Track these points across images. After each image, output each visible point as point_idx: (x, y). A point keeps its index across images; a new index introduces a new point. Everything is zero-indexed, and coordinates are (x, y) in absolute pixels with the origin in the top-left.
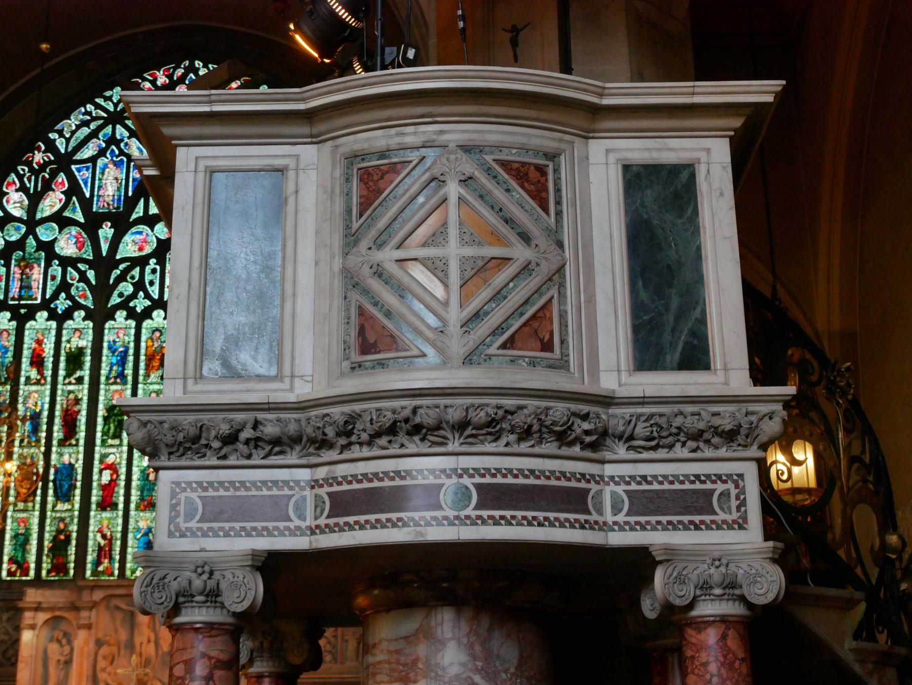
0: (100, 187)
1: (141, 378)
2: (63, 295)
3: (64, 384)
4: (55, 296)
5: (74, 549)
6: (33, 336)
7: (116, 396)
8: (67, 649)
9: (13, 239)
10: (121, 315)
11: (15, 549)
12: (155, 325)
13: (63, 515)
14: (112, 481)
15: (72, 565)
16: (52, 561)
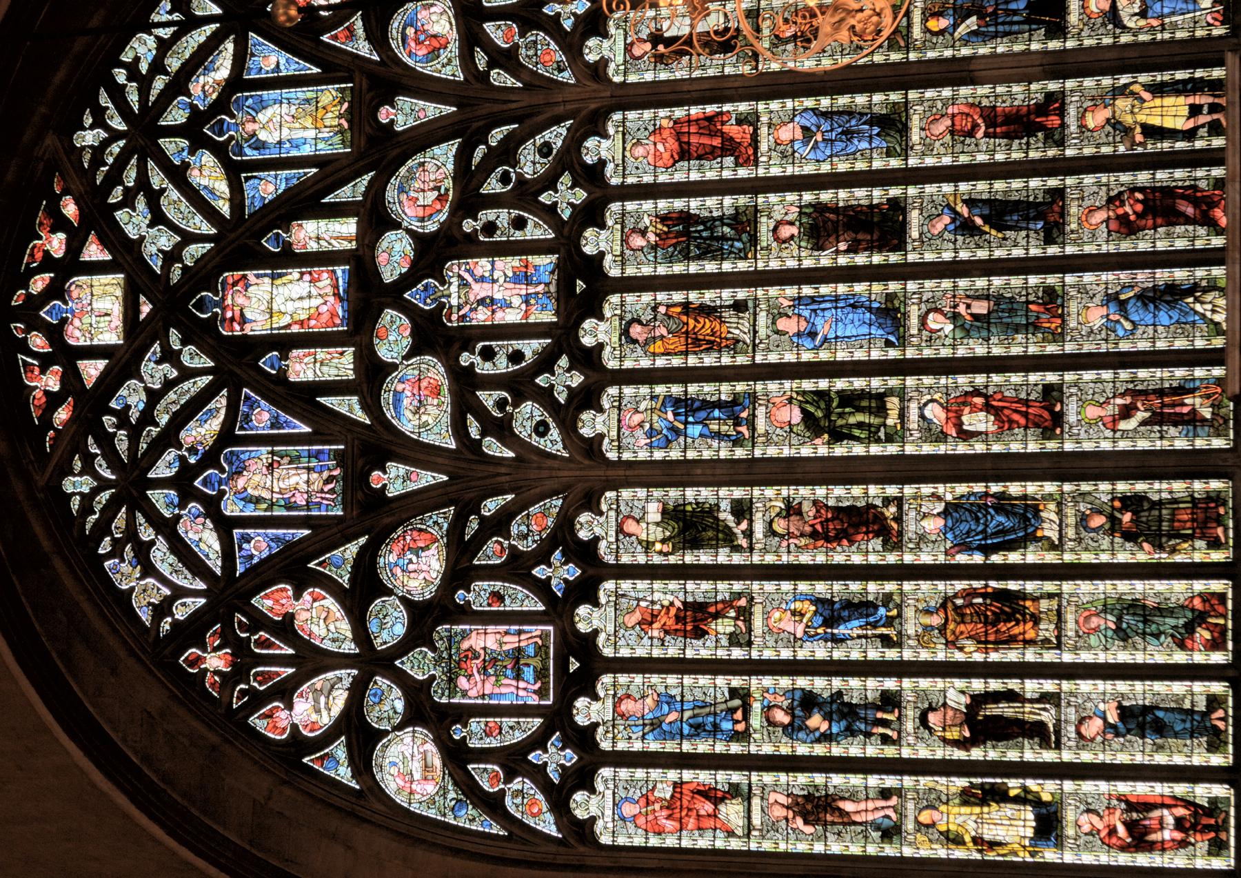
0: (289, 506)
1: (741, 360)
2: (540, 572)
3: (751, 549)
4: (542, 588)
5: (1157, 485)
6: (632, 635)
9: (400, 706)
10: (590, 424)
11: (1157, 636)
12: (615, 339)
13: (1071, 520)
14: (988, 408)
15: (1198, 485)
16: (1186, 538)
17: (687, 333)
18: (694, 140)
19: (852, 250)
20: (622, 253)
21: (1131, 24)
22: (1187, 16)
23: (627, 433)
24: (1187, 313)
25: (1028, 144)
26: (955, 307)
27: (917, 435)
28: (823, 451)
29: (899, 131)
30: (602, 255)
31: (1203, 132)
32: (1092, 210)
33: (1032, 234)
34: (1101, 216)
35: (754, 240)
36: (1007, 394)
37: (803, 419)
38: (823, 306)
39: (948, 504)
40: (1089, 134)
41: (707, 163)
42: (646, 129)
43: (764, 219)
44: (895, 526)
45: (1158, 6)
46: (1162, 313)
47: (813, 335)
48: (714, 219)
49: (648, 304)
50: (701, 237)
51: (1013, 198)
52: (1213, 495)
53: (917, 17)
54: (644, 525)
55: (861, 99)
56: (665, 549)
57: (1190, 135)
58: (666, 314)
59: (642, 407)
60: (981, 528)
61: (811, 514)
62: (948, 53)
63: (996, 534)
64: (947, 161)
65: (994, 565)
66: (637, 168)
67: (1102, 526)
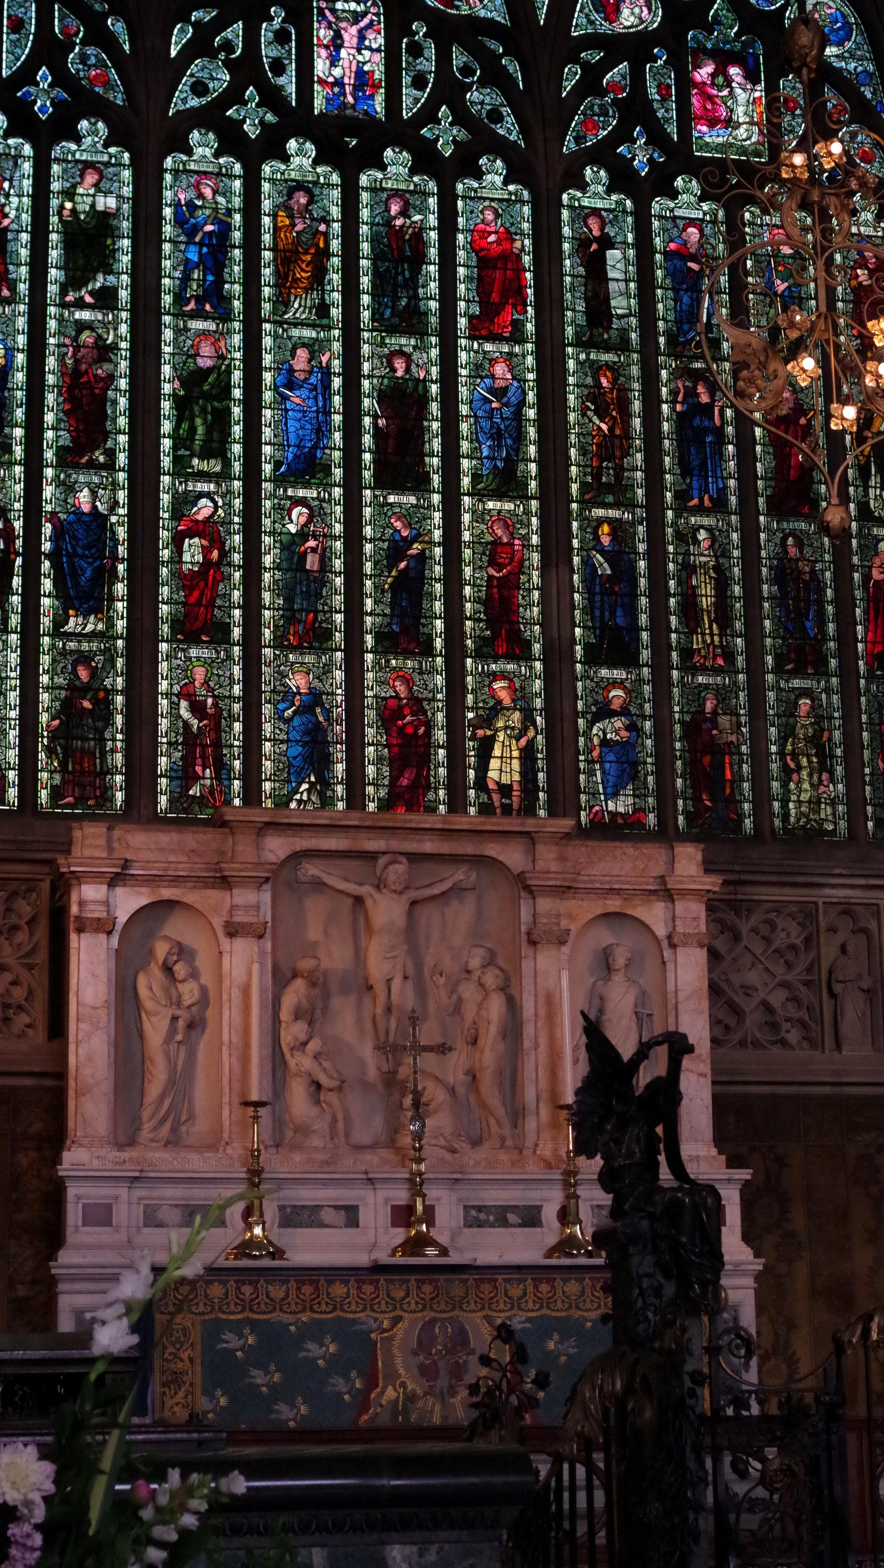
1: (267, 307)
7: (206, 349)
8: (189, 992)
12: (293, 175)
13: (85, 646)
14: (207, 564)
15: (119, 778)
16: (63, 764)
17: (298, 252)
18: (498, 274)
19: (378, 433)
20: (383, 190)
21: (595, 731)
22: (600, 786)
23: (193, 180)
24: (298, 774)
25: (479, 620)
26: (315, 537)
27: (181, 489)
28: (167, 388)
29: (499, 487)
30: (383, 167)
31: (484, 798)
32: (408, 681)
33: (387, 620)
34: (401, 688)
35: (392, 330)
36: (221, 586)
37: (201, 369)
38: (320, 398)
39: (106, 518)
40: (487, 683)
41: (474, 286)
42: (512, 224)
43: (413, 342)
44: (84, 460)
45: (611, 757)
46: (300, 749)
47: (291, 385)
48: (416, 289)
49: (328, 213)
50: (397, 274)
51: (425, 602)
52: (109, 793)
53: (613, 513)
54: (92, 191)
55: (532, 450)
56: (66, 213)
57: (481, 783)
58: (317, 231)
59: (221, 200)
60: (79, 550)
61: (100, 372)
62: (575, 543)
63: (72, 566)
64: (466, 536)
65: (40, 563)
66: (472, 212)
67: (78, 678)
